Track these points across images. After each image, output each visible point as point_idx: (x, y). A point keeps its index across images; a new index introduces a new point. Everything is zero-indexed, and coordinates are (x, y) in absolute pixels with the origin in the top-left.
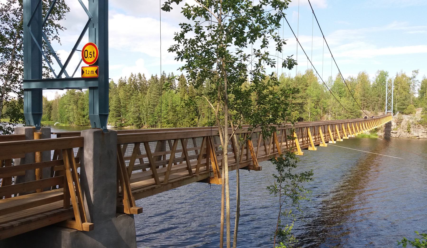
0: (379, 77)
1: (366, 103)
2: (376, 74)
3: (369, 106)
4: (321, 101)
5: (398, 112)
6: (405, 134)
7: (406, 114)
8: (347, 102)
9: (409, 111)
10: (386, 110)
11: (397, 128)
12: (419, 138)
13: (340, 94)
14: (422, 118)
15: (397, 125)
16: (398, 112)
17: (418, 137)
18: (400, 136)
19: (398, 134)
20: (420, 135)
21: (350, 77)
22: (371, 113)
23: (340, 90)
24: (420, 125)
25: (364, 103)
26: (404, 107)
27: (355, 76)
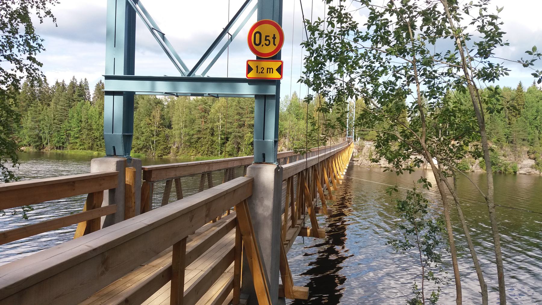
5: (359, 138)
6: (366, 162)
7: (367, 140)
11: (358, 156)
12: (381, 167)
13: (297, 116)
15: (358, 151)
16: (359, 138)
17: (380, 166)
18: (362, 164)
19: (359, 162)
20: (382, 163)
23: (297, 112)
26: (366, 132)
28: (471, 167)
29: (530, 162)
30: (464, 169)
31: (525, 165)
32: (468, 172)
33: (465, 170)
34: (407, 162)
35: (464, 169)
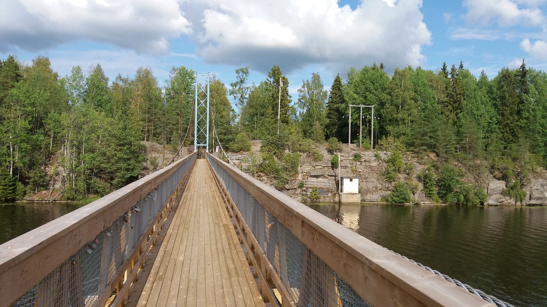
0: (176, 79)
1: (153, 127)
2: (171, 75)
3: (160, 134)
4: (50, 116)
7: (233, 151)
8: (109, 119)
9: (240, 145)
10: (196, 142)
14: (264, 159)
21: (120, 77)
22: (164, 147)
24: (262, 174)
25: (150, 128)
26: (230, 137)
27: (132, 76)
28: (412, 196)
29: (499, 185)
30: (403, 201)
31: (493, 190)
32: (410, 207)
33: (403, 203)
34: (305, 191)
35: (403, 201)
